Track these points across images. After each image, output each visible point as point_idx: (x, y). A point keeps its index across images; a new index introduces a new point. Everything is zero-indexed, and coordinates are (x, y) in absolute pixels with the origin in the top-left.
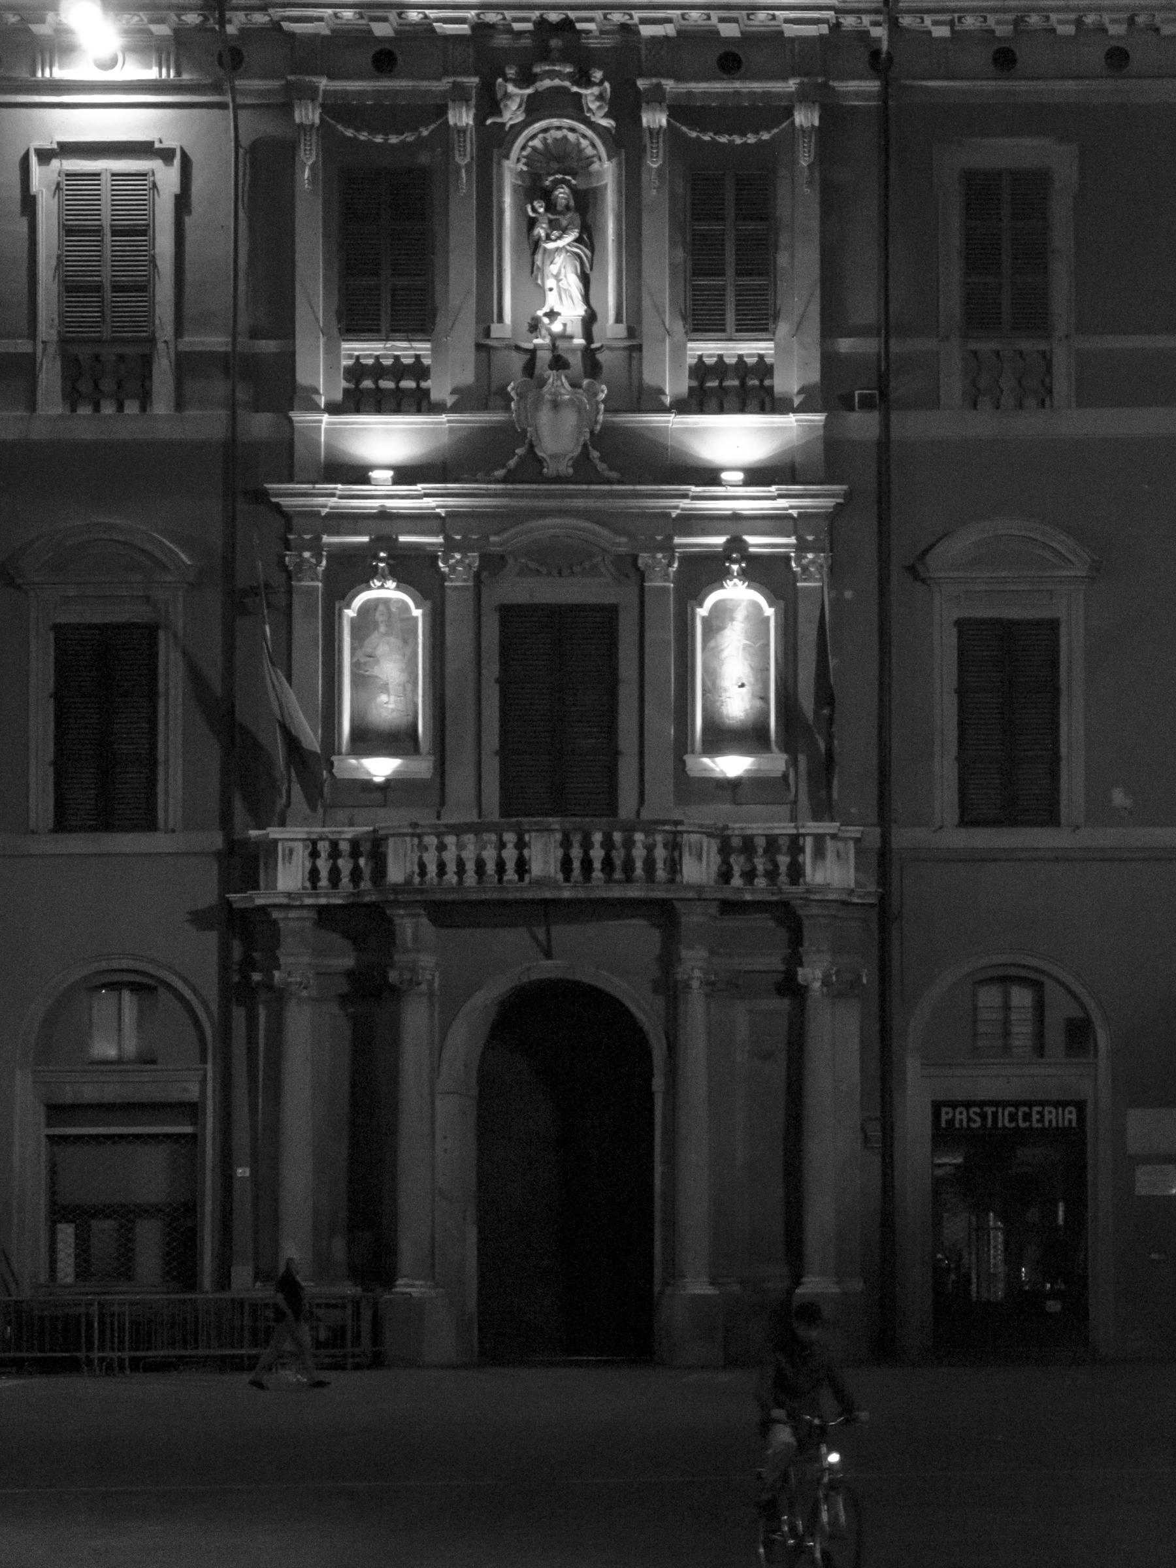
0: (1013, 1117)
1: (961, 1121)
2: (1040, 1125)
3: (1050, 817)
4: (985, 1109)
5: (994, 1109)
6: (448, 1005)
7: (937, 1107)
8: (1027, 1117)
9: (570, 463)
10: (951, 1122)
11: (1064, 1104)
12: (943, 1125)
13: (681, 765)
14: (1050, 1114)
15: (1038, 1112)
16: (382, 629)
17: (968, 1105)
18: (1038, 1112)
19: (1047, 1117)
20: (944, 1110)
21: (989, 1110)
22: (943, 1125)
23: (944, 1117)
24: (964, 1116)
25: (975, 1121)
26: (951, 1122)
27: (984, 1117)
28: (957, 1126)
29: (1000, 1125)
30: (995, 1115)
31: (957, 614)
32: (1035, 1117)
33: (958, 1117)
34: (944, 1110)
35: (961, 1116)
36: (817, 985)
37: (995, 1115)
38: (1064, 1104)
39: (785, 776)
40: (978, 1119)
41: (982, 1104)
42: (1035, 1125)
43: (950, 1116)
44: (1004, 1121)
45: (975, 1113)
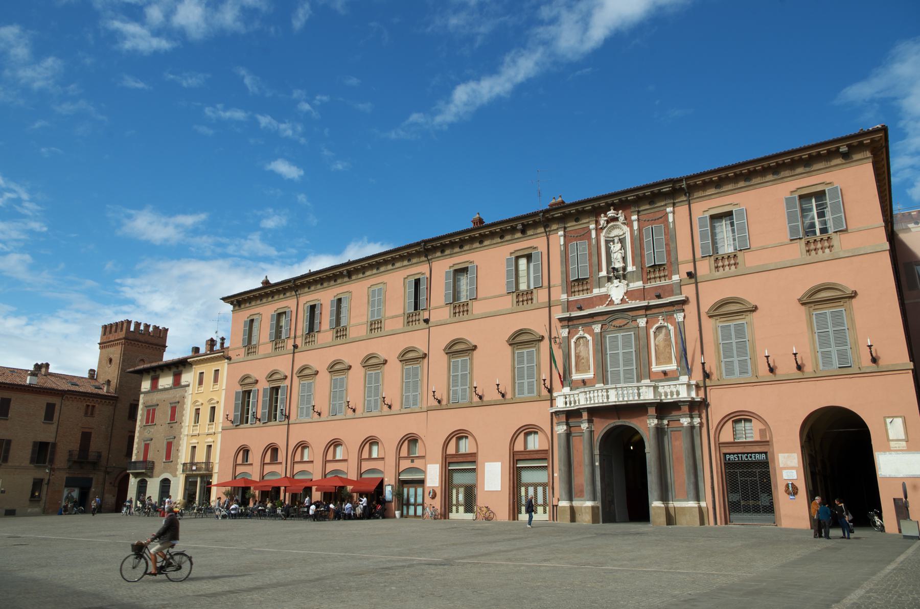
11: (761, 453)
13: (649, 369)
14: (757, 456)
17: (734, 454)
35: (732, 457)
38: (761, 453)
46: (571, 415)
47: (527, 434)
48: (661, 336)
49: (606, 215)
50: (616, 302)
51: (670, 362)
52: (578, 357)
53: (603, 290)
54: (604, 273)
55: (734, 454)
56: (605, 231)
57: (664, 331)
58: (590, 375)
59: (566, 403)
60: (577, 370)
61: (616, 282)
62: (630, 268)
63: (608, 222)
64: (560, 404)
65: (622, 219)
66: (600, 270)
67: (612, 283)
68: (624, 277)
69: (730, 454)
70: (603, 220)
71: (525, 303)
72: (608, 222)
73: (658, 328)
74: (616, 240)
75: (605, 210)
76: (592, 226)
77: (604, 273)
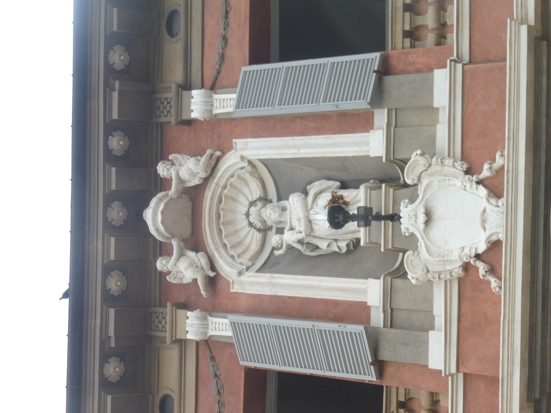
9: (493, 201)
49: (163, 250)
50: (496, 226)
53: (441, 305)
54: (371, 291)
56: (226, 269)
61: (410, 217)
62: (372, 144)
63: (195, 243)
66: (356, 312)
67: (412, 242)
68: (390, 175)
70: (182, 268)
72: (195, 243)
74: (270, 214)
75: (140, 250)
76: (191, 326)
77: (371, 291)
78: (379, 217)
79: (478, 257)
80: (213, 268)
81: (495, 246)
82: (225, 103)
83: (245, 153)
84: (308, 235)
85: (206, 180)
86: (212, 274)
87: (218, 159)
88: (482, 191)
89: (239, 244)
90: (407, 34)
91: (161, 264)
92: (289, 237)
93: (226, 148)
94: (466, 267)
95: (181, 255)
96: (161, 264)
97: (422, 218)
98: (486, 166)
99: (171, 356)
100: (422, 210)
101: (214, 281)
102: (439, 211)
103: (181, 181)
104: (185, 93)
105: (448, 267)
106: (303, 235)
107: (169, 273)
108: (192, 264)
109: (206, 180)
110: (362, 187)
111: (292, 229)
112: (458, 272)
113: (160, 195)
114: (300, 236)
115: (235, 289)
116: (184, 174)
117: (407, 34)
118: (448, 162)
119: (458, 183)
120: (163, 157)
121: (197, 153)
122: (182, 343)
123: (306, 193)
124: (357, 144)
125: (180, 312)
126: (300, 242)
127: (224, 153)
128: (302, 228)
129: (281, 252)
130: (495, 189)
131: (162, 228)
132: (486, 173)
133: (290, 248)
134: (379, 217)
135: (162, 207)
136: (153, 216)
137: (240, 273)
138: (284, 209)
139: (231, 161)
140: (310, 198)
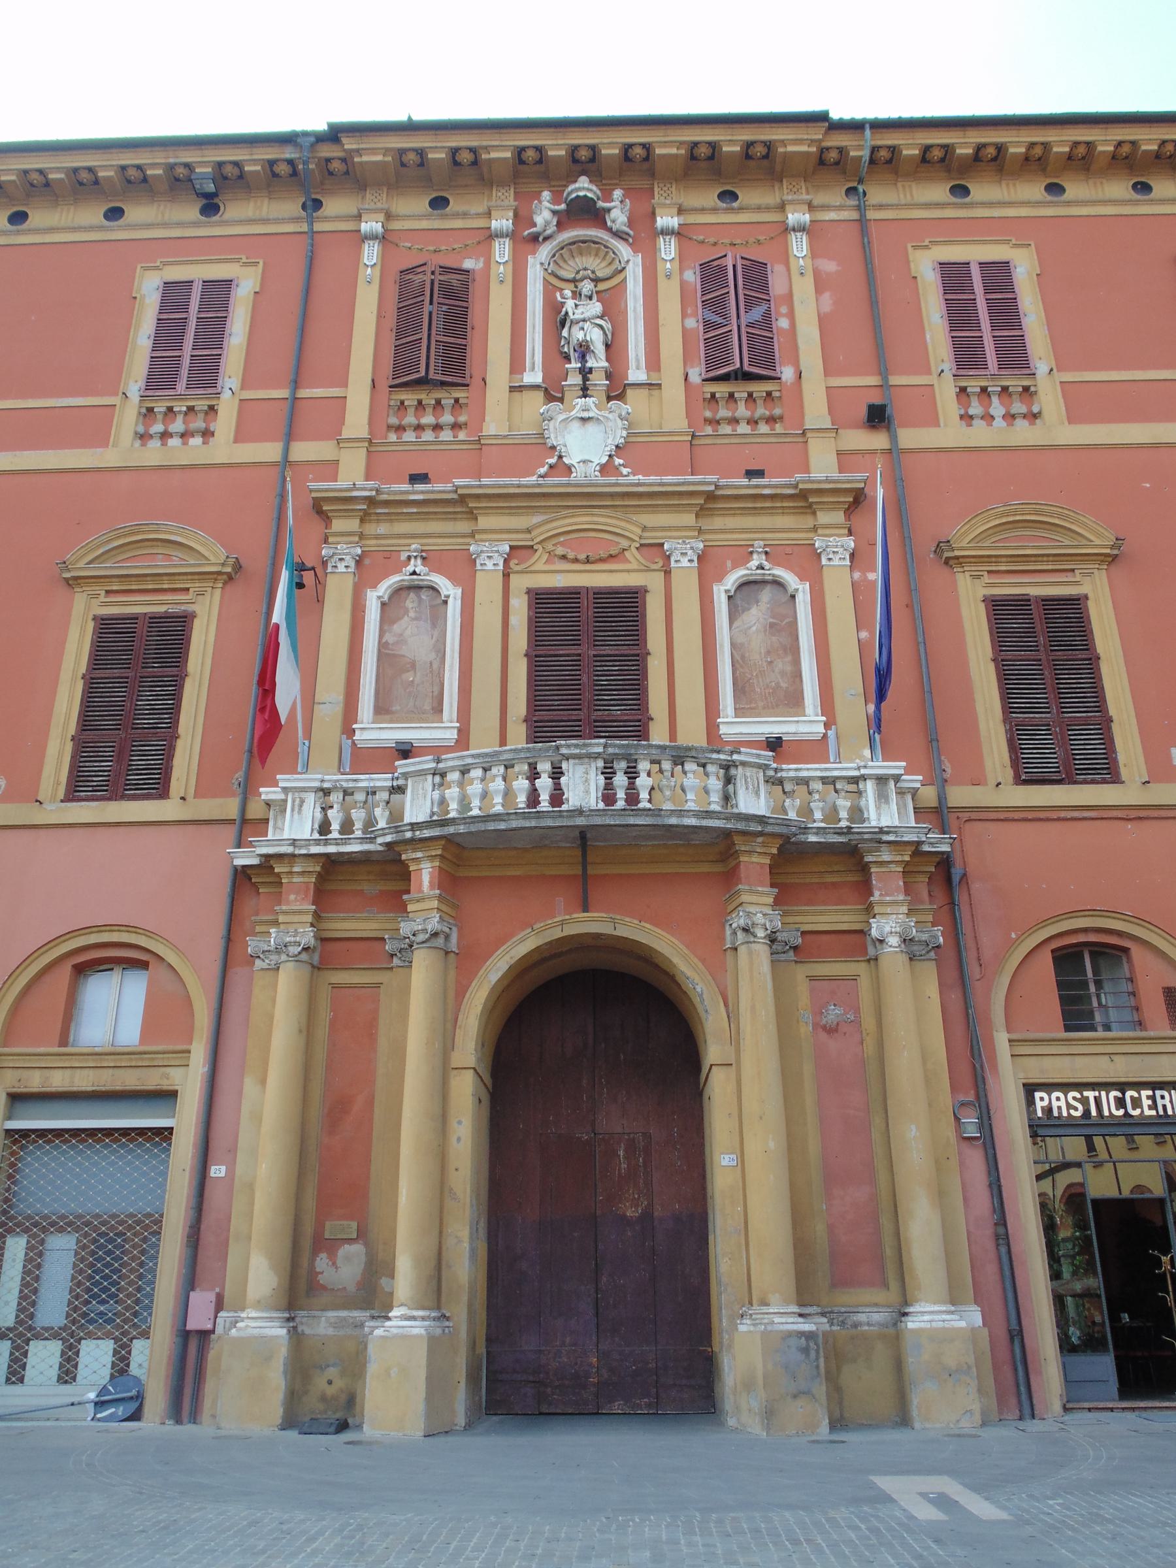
0: (1121, 1103)
1: (1059, 1108)
2: (1153, 1113)
3: (1109, 772)
4: (1086, 1094)
5: (1097, 1094)
6: (462, 961)
7: (1030, 1089)
8: (1136, 1103)
9: (598, 468)
10: (1048, 1110)
12: (1040, 1114)
15: (1148, 1097)
16: (412, 614)
18: (1148, 1097)
19: (1160, 1102)
20: (1038, 1095)
21: (1090, 1095)
22: (1040, 1114)
23: (1039, 1105)
24: (1062, 1103)
25: (1076, 1109)
26: (1048, 1110)
27: (1084, 1101)
28: (1056, 1114)
29: (1106, 1113)
30: (1098, 1101)
31: (983, 592)
32: (1146, 1103)
33: (1055, 1104)
34: (1038, 1095)
36: (894, 941)
37: (1098, 1101)
39: (825, 736)
40: (1080, 1107)
41: (1080, 1086)
42: (1148, 1112)
43: (1045, 1103)
44: (1110, 1107)
45: (1074, 1098)
46: (361, 877)
47: (82, 970)
48: (756, 615)
51: (793, 701)
52: (385, 655)
55: (1065, 1087)
56: (545, 252)
57: (766, 594)
58: (444, 732)
59: (324, 828)
60: (382, 710)
64: (296, 827)
65: (618, 217)
68: (617, 391)
69: (1049, 1087)
71: (174, 442)
73: (745, 585)
76: (502, 222)
78: (585, 379)
79: (560, 457)
80: (546, 239)
81: (569, 469)
82: (668, 250)
83: (631, 263)
84: (572, 322)
85: (610, 230)
86: (541, 239)
87: (626, 240)
88: (604, 459)
89: (565, 261)
90: (713, 395)
91: (546, 195)
92: (570, 304)
93: (635, 247)
94: (553, 448)
95: (554, 212)
96: (546, 195)
97: (585, 415)
98: (621, 462)
99: (479, 208)
100: (591, 414)
101: (535, 239)
102: (591, 427)
103: (609, 210)
104: (675, 211)
105: (552, 436)
106: (572, 317)
107: (540, 202)
108: (547, 223)
109: (610, 230)
110: (606, 364)
111: (576, 306)
112: (549, 443)
113: (598, 192)
114: (570, 314)
115: (530, 259)
116: (615, 213)
117: (713, 395)
118: (624, 433)
119: (610, 441)
120: (628, 193)
121: (631, 222)
122: (489, 214)
123: (601, 317)
124: (638, 360)
125: (511, 214)
126: (567, 313)
127: (630, 245)
128: (576, 316)
129: (559, 298)
130: (604, 469)
131: (574, 196)
132: (618, 461)
133: (563, 304)
134: (585, 379)
135: (590, 195)
136: (583, 187)
137: (542, 264)
138: (590, 298)
139: (624, 250)
140: (599, 321)
